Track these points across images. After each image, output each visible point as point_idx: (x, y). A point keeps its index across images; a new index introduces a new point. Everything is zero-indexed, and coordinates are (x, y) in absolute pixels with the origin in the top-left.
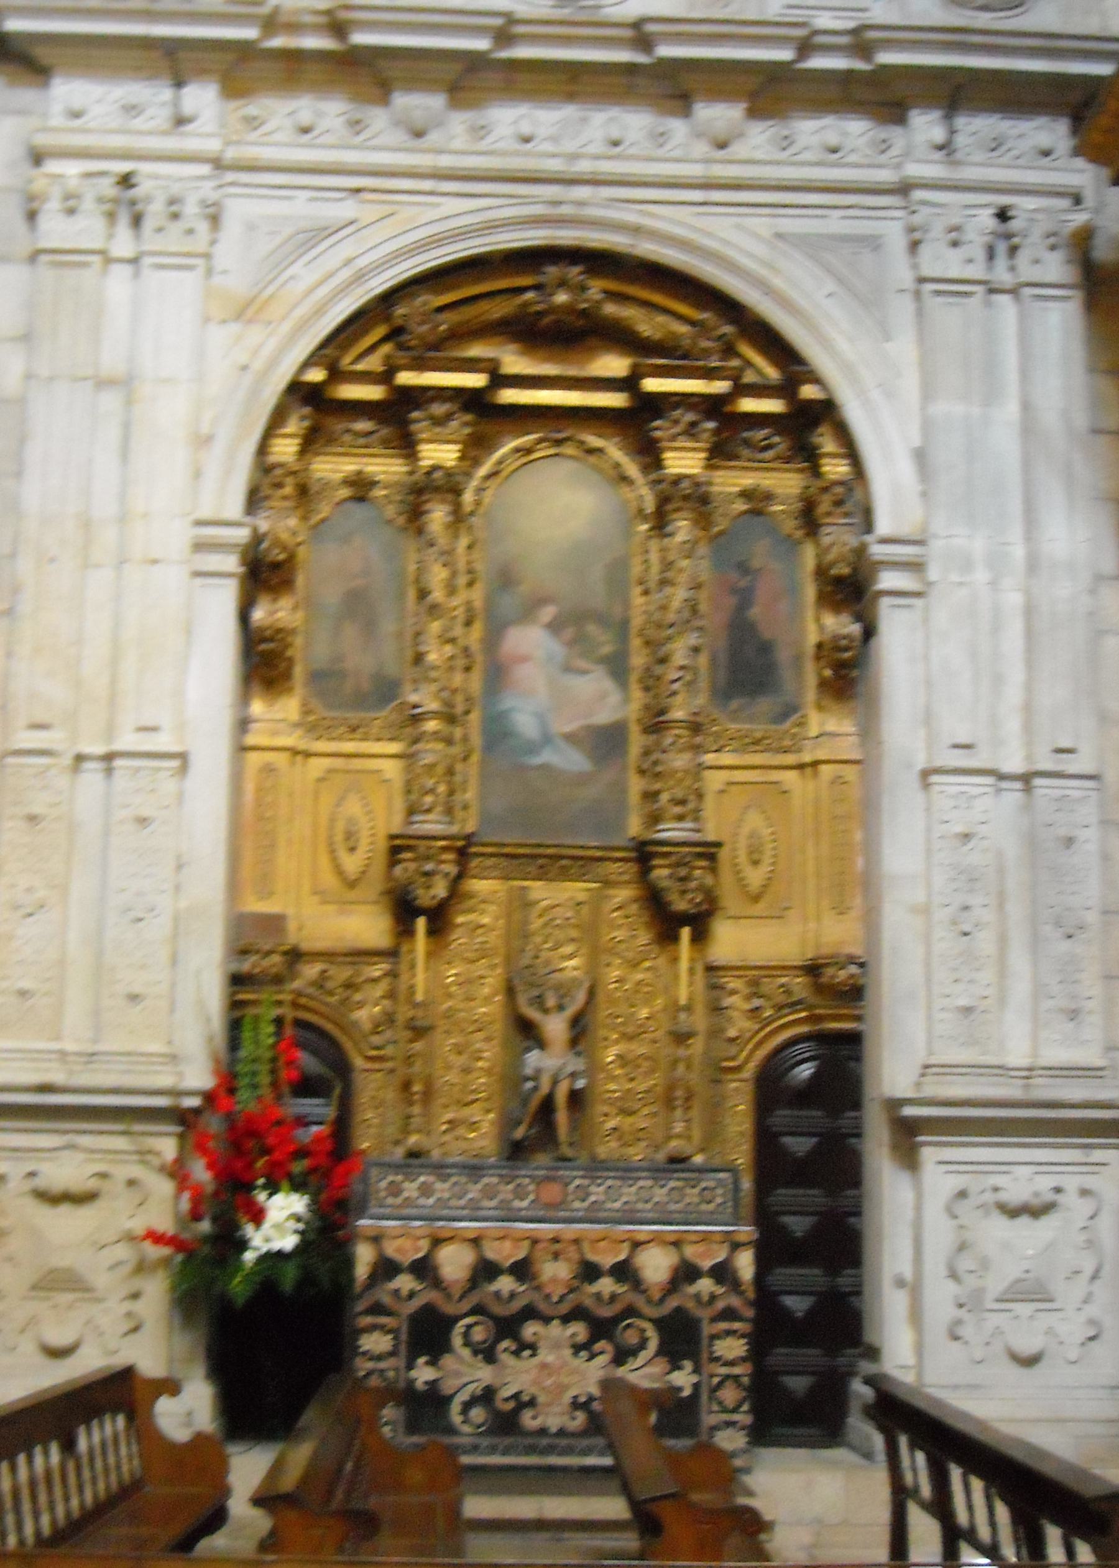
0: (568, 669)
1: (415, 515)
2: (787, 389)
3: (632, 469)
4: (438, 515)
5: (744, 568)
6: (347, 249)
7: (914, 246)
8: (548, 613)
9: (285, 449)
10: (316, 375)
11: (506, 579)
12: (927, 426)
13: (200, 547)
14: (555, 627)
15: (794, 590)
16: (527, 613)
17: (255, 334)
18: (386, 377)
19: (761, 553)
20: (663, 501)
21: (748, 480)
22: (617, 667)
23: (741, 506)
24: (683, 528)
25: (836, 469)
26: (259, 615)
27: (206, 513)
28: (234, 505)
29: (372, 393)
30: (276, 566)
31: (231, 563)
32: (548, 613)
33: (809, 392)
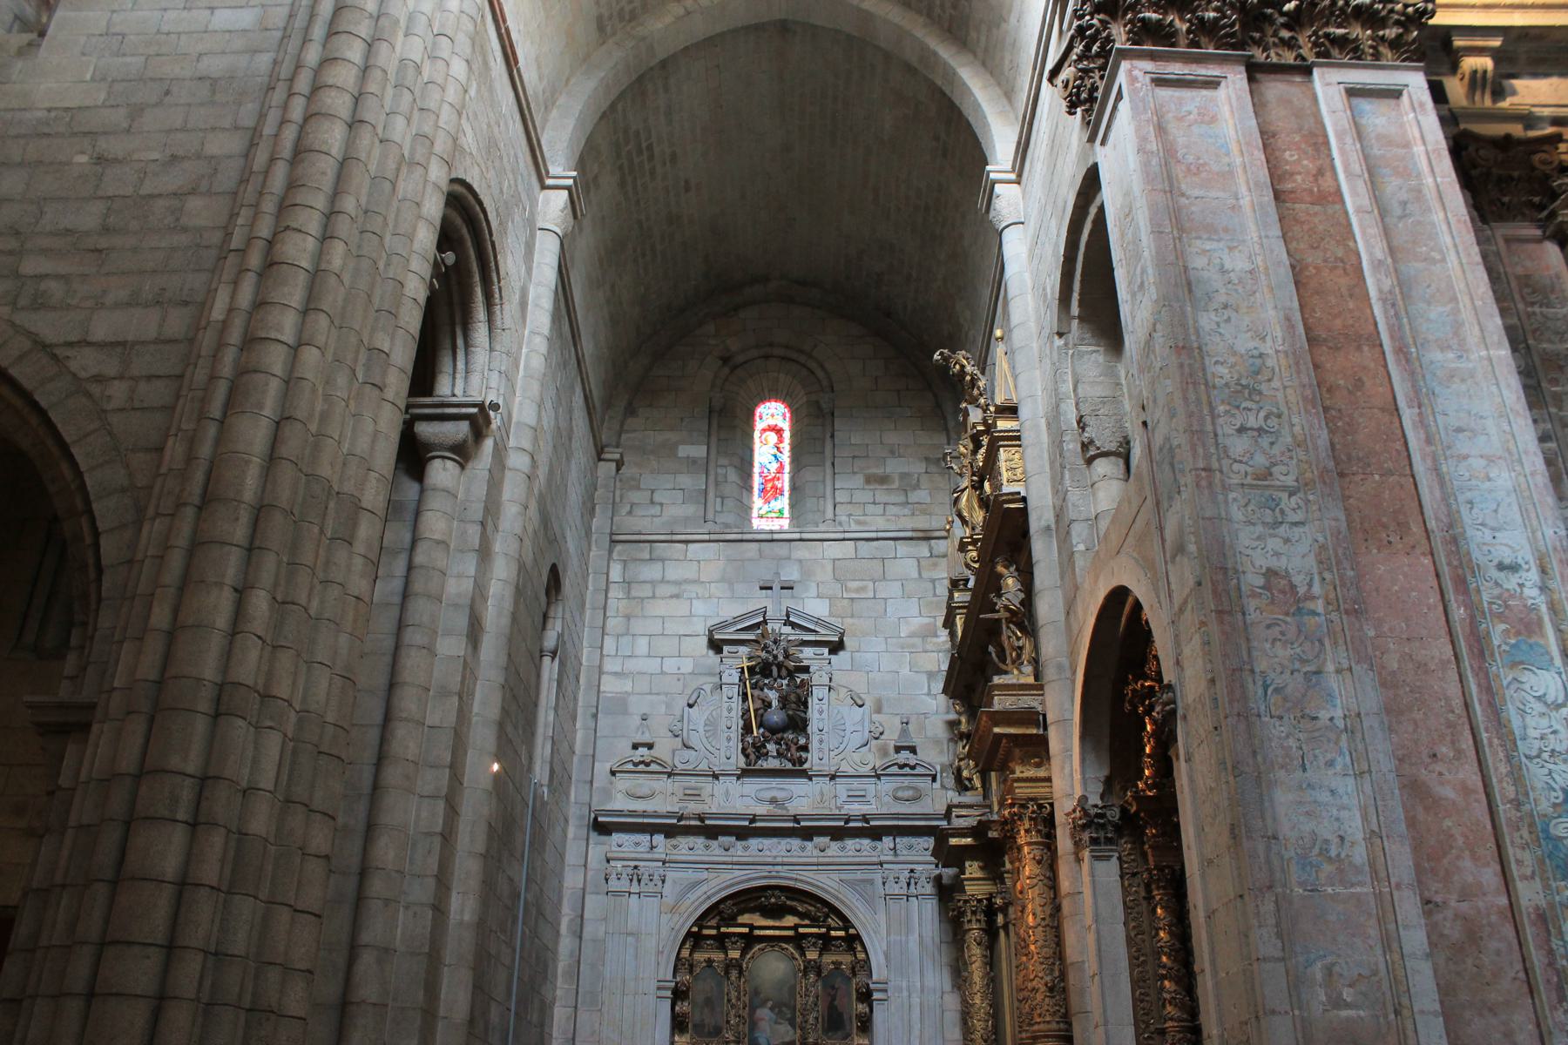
0: (776, 1023)
1: (727, 973)
2: (846, 929)
3: (797, 956)
4: (734, 974)
5: (833, 987)
6: (704, 888)
7: (884, 883)
8: (770, 1004)
9: (685, 953)
10: (695, 929)
11: (756, 992)
12: (888, 943)
13: (659, 988)
14: (772, 1009)
15: (850, 995)
16: (763, 1004)
17: (676, 918)
18: (718, 928)
19: (838, 982)
20: (805, 968)
21: (834, 958)
22: (792, 1023)
23: (832, 967)
24: (812, 977)
25: (861, 956)
26: (677, 1008)
27: (661, 977)
28: (669, 976)
29: (714, 932)
30: (683, 992)
31: (669, 994)
32: (770, 1004)
33: (852, 931)
